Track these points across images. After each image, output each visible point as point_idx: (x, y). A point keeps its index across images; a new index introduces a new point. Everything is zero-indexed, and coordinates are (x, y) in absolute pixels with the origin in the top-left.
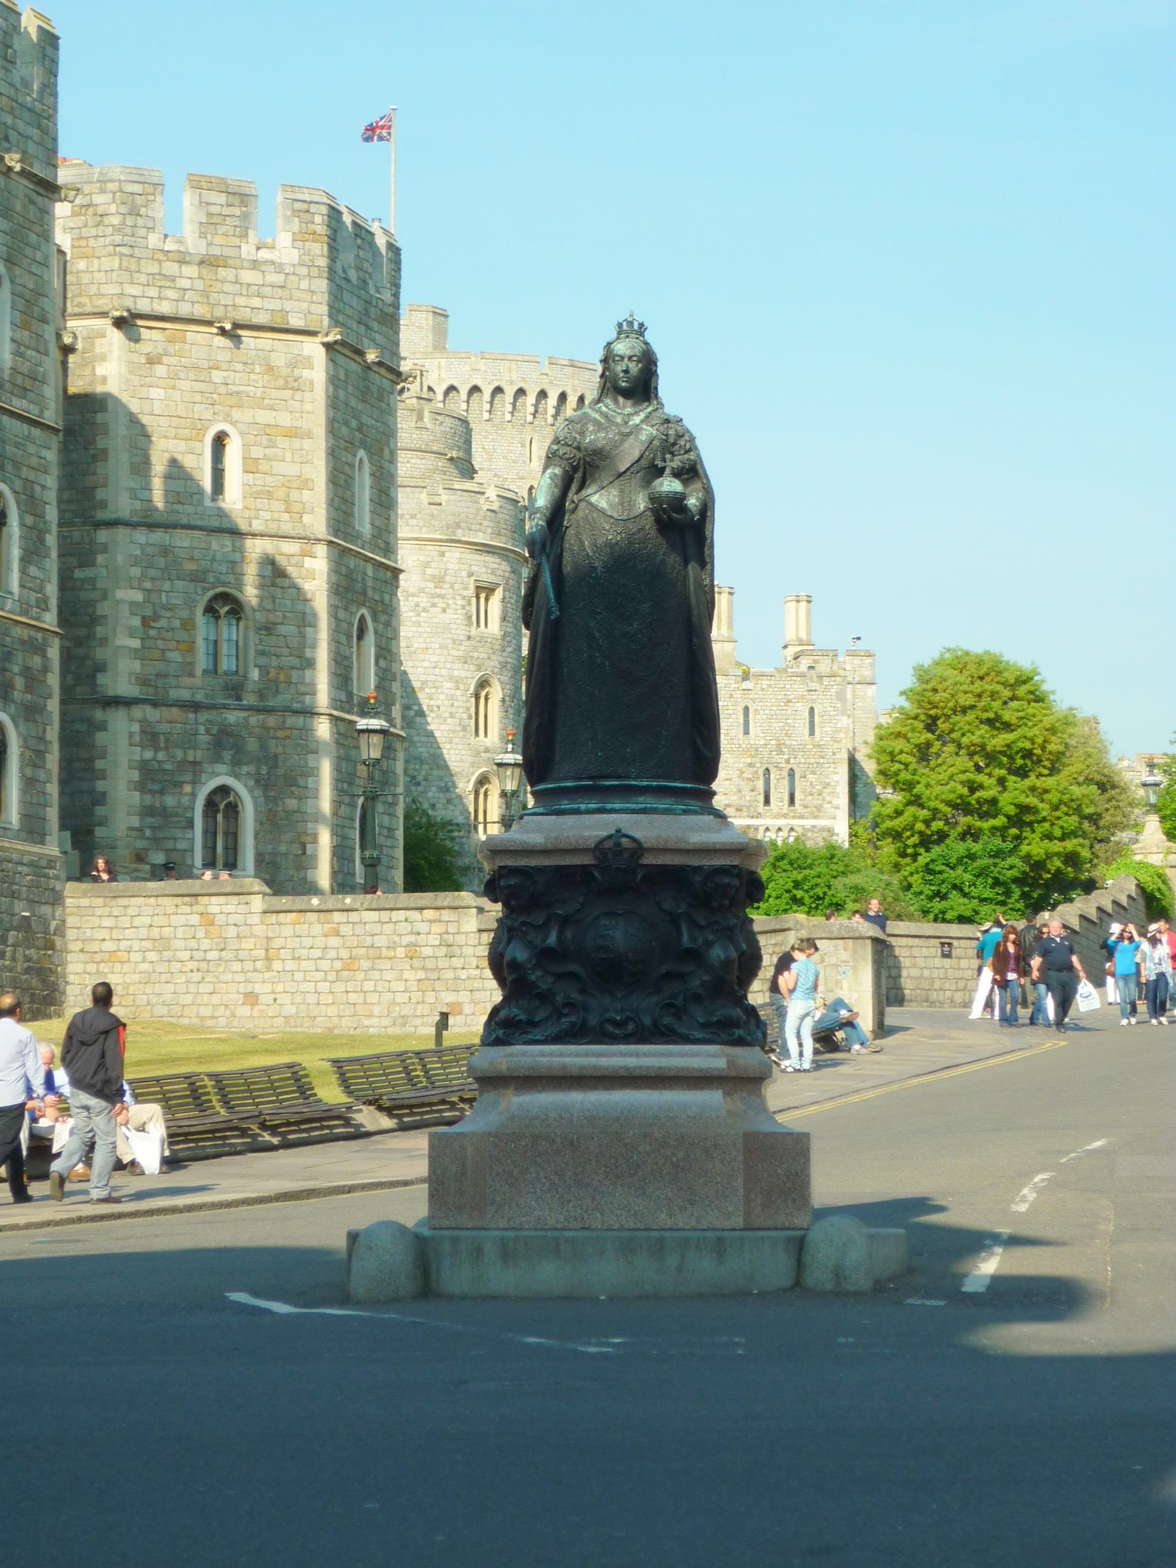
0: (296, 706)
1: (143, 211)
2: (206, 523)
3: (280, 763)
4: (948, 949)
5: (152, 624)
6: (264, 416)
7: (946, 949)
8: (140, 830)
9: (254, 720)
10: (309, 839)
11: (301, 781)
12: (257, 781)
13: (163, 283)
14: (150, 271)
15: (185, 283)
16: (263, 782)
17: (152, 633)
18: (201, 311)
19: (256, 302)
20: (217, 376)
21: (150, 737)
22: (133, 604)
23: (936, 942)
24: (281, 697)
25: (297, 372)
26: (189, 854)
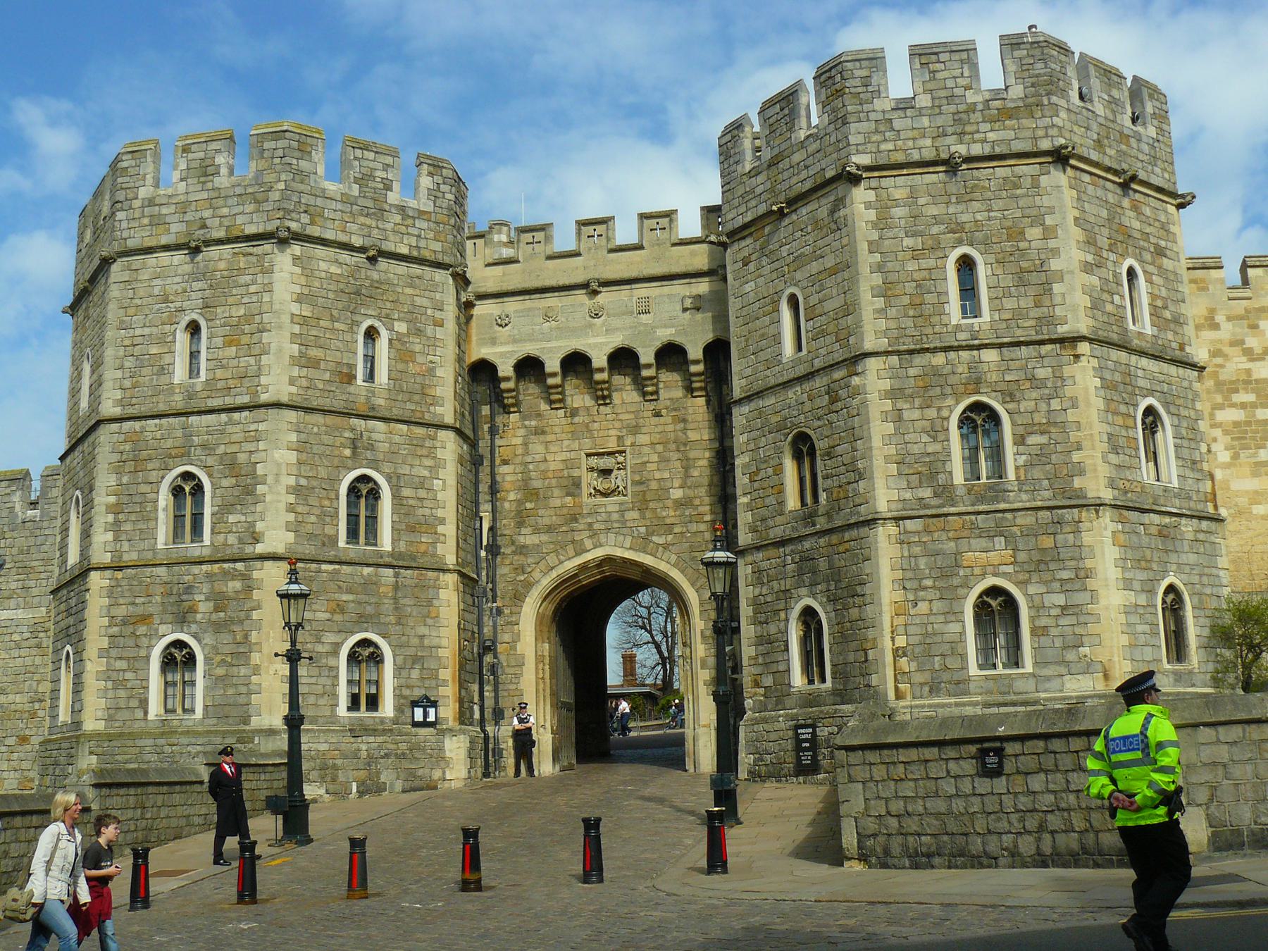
1: (732, 152)
2: (785, 378)
4: (996, 759)
6: (815, 267)
7: (992, 760)
8: (756, 658)
9: (822, 540)
10: (869, 645)
11: (859, 589)
13: (747, 198)
14: (740, 194)
15: (759, 190)
17: (756, 485)
19: (804, 174)
22: (745, 466)
23: (973, 749)
24: (842, 513)
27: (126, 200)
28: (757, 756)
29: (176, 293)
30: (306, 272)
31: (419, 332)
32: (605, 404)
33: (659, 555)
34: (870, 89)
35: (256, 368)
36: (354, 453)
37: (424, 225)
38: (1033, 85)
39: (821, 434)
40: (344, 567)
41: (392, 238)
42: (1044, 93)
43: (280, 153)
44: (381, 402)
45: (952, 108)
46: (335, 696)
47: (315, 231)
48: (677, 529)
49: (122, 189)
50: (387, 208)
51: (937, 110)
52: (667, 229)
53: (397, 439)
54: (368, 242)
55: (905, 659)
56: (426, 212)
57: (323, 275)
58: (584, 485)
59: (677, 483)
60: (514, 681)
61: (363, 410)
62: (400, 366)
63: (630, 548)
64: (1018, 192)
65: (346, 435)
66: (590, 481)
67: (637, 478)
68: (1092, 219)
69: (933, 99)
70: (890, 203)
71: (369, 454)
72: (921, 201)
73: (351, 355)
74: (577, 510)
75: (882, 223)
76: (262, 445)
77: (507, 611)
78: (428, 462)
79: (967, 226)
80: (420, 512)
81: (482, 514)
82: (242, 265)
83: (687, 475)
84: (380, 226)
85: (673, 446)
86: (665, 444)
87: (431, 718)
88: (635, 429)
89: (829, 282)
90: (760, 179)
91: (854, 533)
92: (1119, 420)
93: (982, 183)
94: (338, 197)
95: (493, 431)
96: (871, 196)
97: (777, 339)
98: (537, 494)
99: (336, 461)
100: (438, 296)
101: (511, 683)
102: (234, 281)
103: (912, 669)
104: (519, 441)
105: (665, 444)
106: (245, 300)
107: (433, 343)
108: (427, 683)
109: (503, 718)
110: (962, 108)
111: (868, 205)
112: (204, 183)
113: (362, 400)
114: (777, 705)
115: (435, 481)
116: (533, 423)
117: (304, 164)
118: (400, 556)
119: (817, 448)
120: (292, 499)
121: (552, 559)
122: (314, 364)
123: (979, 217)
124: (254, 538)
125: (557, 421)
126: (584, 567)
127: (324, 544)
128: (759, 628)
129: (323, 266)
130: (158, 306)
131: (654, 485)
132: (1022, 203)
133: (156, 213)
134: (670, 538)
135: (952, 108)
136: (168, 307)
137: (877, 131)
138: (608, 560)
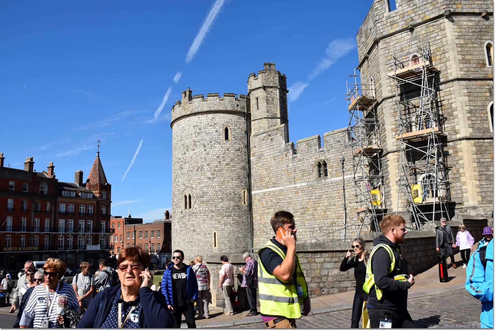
35: (445, 67)
76: (453, 96)
82: (431, 30)
102: (429, 37)
130: (399, 53)
136: (403, 53)
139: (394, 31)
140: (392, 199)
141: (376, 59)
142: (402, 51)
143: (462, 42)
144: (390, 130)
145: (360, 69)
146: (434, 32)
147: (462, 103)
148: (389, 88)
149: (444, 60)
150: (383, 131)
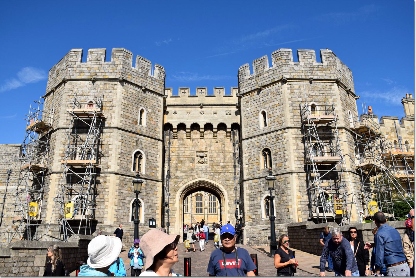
0: (284, 172)
1: (244, 73)
2: (261, 133)
3: (281, 188)
5: (250, 160)
6: (271, 104)
10: (289, 207)
11: (286, 191)
12: (275, 193)
14: (246, 84)
15: (253, 83)
16: (277, 194)
17: (250, 162)
18: (256, 87)
19: (268, 80)
20: (261, 99)
21: (251, 187)
22: (246, 157)
24: (280, 170)
25: (278, 91)
26: (260, 215)
27: (72, 65)
28: (250, 238)
29: (86, 93)
30: (127, 91)
31: (154, 113)
32: (202, 138)
33: (216, 181)
34: (288, 59)
35: (111, 117)
36: (136, 145)
37: (157, 83)
38: (329, 63)
39: (273, 149)
40: (133, 178)
41: (149, 85)
42: (332, 65)
43: (121, 57)
44: (144, 131)
45: (309, 66)
46: (128, 216)
47: (129, 80)
48: (222, 174)
49: (70, 61)
50: (148, 77)
51: (305, 66)
52: (222, 92)
53: (148, 142)
54: (143, 85)
55: (300, 211)
56: (157, 80)
57: (131, 93)
58: (195, 160)
59: (222, 161)
60: (173, 215)
61: (139, 132)
62: (149, 122)
63: (208, 179)
64: (326, 89)
65: (135, 139)
66: (197, 159)
67: (211, 159)
68: (343, 98)
69: (304, 63)
70: (294, 89)
71: (140, 145)
72: (302, 89)
73: (137, 116)
74: (193, 167)
75: (292, 93)
76: (111, 139)
77: (172, 194)
78: (155, 150)
79: (314, 97)
80: (153, 164)
81: (165, 166)
82: (108, 87)
83: (225, 159)
84: (146, 81)
85: (221, 151)
86: (219, 150)
87: (154, 224)
88: (210, 146)
89: (276, 108)
90: (253, 80)
91: (285, 176)
92: (351, 150)
93: (317, 86)
94: (135, 71)
95: (170, 143)
96: (289, 86)
97: (258, 123)
98: (182, 163)
99: (132, 146)
100: (159, 103)
101: (172, 215)
103: (302, 214)
104: (177, 146)
105: (219, 150)
106: (108, 97)
107: (158, 116)
108: (153, 214)
109: (170, 226)
110: (312, 66)
111: (288, 89)
112: (97, 63)
113: (139, 129)
114: (257, 223)
115: (157, 155)
116: (181, 142)
117: (127, 61)
118: (147, 176)
119: (271, 152)
120: (119, 156)
121: (186, 181)
122: (127, 118)
123: (317, 94)
124: (108, 167)
125: (188, 142)
126: (194, 183)
127: (127, 171)
128: (251, 202)
129: (131, 90)
130: (80, 96)
131: (215, 161)
132: (328, 92)
133: (81, 69)
134: (220, 176)
135: (309, 66)
136: (83, 97)
137: (290, 70)
138: (202, 182)
139: (80, 78)
140: (47, 212)
141: (61, 95)
142: (83, 95)
143: (126, 102)
144: (58, 155)
145: (45, 99)
146: (109, 89)
147: (116, 146)
148: (65, 121)
149: (111, 111)
150: (52, 154)
